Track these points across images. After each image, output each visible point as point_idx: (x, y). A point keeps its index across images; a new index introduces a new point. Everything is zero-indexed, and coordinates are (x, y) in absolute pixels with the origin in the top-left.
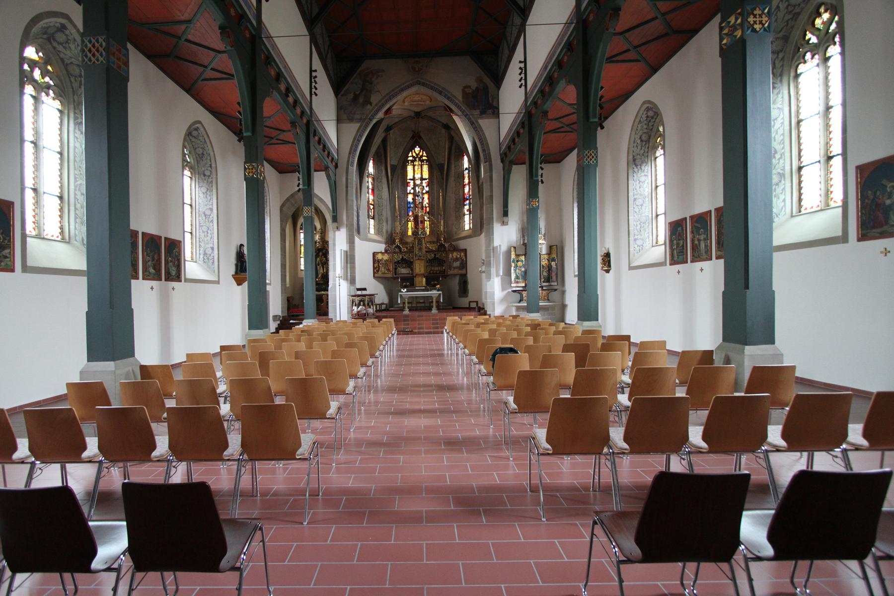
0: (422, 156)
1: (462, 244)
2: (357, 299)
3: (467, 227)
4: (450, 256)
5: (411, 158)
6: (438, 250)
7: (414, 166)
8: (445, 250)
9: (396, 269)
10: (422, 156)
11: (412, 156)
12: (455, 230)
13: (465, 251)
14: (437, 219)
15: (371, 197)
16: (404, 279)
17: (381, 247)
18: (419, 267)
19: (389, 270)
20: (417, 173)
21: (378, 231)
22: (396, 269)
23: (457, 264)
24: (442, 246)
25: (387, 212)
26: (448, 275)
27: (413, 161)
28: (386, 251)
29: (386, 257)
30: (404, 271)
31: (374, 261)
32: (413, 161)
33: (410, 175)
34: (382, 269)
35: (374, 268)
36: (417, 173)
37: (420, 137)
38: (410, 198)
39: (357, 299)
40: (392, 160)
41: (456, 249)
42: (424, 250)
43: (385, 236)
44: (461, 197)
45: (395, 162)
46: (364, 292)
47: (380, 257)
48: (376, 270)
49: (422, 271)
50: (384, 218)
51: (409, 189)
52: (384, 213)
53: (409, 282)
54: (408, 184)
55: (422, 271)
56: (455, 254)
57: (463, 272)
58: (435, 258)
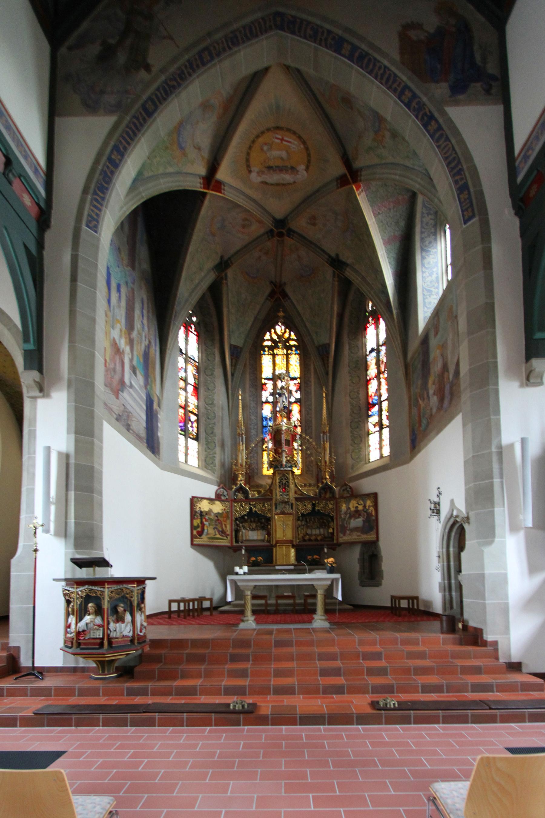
0: (289, 339)
1: (367, 485)
2: (82, 590)
3: (374, 456)
4: (344, 507)
5: (269, 343)
6: (319, 497)
7: (274, 355)
8: (333, 497)
9: (237, 531)
10: (289, 339)
11: (272, 340)
12: (350, 461)
13: (374, 496)
14: (318, 439)
15: (193, 402)
16: (252, 550)
17: (210, 490)
18: (283, 528)
19: (223, 532)
20: (281, 365)
21: (206, 461)
22: (237, 531)
23: (358, 522)
24: (327, 488)
25: (223, 429)
26: (339, 545)
27: (271, 348)
28: (218, 497)
29: (218, 507)
30: (254, 536)
31: (193, 513)
33: (267, 371)
34: (209, 530)
35: (193, 527)
36: (281, 365)
38: (267, 410)
39: (82, 590)
41: (354, 495)
42: (292, 495)
44: (362, 402)
45: (238, 341)
46: (100, 573)
47: (204, 506)
48: (197, 531)
49: (289, 535)
50: (217, 439)
53: (262, 557)
54: (262, 387)
55: (289, 535)
56: (353, 504)
57: (371, 537)
58: (314, 513)
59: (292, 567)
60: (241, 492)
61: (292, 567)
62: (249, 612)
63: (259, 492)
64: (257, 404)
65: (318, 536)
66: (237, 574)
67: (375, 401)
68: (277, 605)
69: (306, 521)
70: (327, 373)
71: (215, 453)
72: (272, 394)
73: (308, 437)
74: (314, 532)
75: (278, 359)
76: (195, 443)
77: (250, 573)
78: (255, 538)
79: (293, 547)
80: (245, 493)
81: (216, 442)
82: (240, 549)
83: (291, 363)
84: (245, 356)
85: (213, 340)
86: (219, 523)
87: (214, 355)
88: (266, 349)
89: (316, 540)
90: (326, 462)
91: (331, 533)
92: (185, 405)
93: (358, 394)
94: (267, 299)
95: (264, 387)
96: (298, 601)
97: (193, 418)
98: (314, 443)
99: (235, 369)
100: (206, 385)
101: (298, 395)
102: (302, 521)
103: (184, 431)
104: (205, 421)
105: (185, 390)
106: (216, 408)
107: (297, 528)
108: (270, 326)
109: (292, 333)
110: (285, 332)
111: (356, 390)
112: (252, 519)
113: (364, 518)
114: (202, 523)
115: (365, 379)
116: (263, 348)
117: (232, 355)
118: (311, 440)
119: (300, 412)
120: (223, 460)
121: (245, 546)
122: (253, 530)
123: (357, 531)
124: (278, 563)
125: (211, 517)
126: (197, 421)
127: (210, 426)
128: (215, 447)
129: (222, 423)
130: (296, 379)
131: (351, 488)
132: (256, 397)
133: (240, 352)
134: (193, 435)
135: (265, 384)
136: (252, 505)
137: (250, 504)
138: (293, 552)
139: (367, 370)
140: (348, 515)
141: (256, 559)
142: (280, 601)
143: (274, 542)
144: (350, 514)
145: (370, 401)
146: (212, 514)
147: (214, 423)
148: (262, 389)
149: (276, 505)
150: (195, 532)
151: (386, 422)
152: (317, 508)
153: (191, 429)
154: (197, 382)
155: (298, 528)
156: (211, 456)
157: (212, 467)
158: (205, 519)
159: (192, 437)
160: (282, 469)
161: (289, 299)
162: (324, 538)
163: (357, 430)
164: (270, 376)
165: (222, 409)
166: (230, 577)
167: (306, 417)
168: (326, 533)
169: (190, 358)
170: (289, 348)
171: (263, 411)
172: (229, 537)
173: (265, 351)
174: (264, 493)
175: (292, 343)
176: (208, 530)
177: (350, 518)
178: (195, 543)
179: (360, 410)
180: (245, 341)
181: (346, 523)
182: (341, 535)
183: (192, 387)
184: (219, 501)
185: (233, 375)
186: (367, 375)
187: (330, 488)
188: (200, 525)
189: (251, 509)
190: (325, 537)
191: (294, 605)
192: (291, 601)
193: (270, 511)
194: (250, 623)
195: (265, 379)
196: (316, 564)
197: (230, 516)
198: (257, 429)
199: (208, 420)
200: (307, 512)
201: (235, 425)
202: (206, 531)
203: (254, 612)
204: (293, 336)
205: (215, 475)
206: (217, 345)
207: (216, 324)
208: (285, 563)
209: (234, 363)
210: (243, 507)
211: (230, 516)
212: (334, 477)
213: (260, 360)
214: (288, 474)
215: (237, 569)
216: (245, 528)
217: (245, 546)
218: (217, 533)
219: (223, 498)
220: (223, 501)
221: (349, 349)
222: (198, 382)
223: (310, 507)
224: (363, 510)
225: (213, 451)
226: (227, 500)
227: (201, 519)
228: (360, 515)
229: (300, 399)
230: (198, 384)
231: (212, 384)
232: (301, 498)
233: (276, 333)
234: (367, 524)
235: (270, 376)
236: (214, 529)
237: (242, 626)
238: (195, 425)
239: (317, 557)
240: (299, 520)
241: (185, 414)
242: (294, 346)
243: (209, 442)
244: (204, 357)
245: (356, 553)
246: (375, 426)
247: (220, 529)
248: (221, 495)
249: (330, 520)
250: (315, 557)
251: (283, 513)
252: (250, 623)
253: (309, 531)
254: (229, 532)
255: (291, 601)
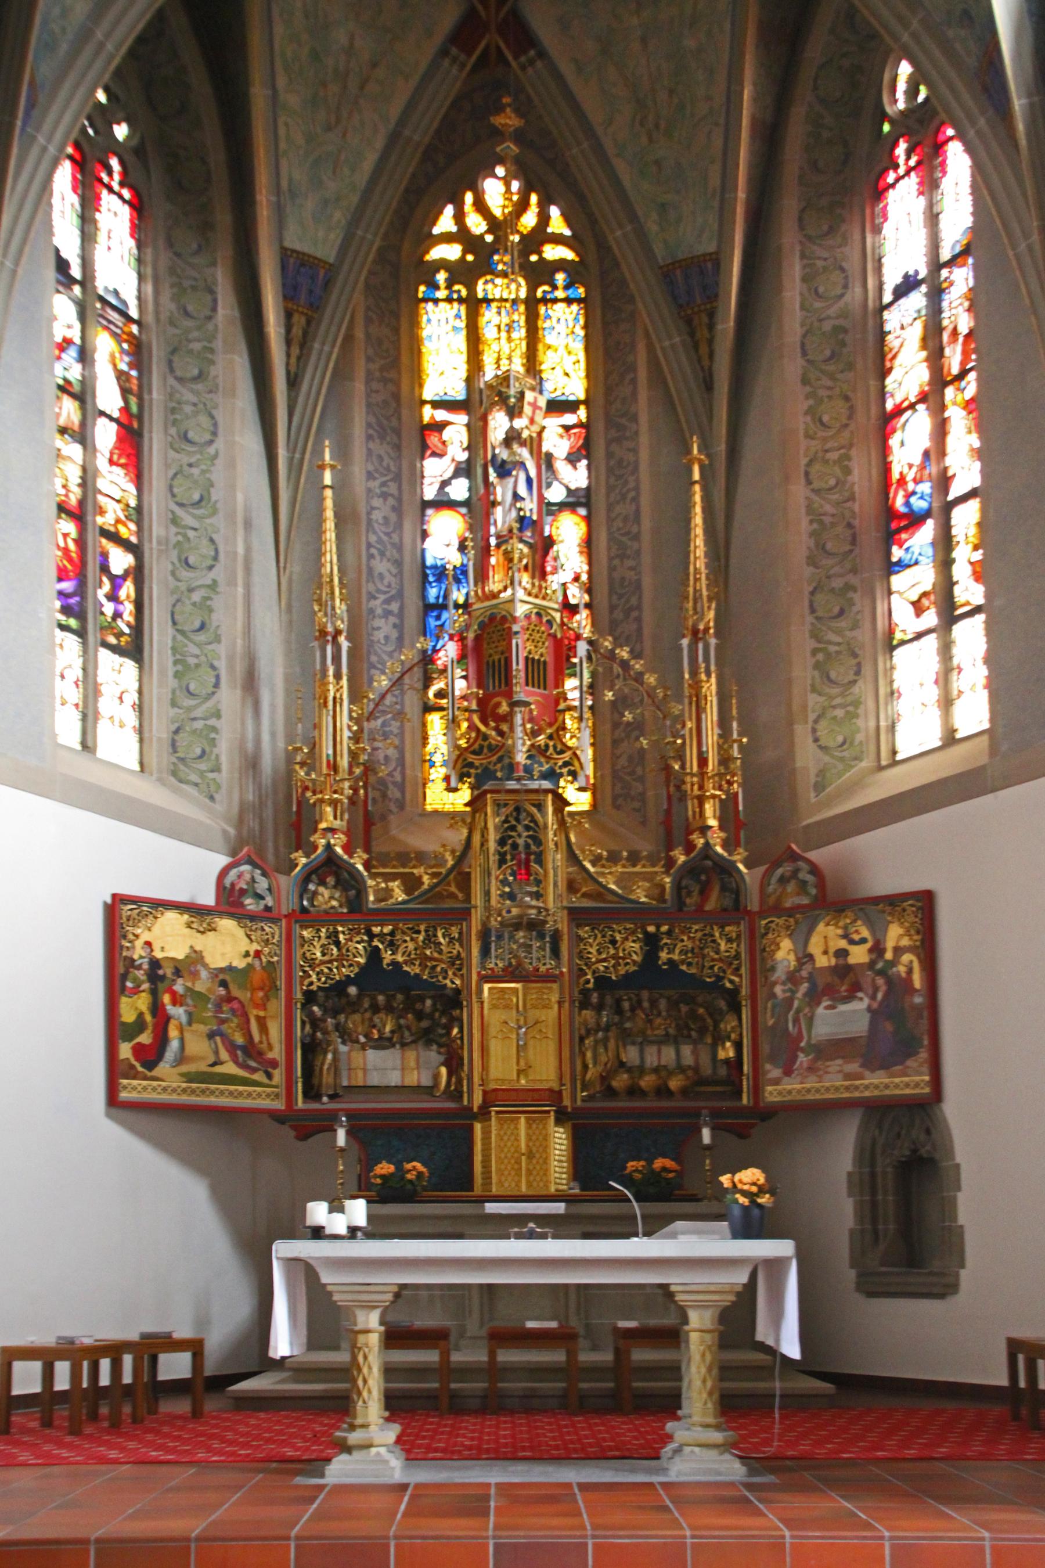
0: (539, 236)
1: (885, 860)
3: (916, 731)
4: (785, 953)
5: (452, 252)
6: (674, 910)
7: (474, 305)
8: (735, 909)
10: (539, 236)
11: (462, 236)
14: (668, 661)
17: (194, 870)
19: (250, 1053)
21: (177, 750)
23: (848, 1017)
24: (708, 871)
26: (765, 1114)
27: (460, 273)
28: (230, 900)
29: (228, 945)
32: (463, 274)
34: (191, 1041)
35: (115, 1030)
36: (505, 351)
37: (523, 38)
38: (444, 538)
40: (303, 211)
41: (832, 900)
42: (553, 901)
43: (228, 801)
44: (865, 503)
48: (133, 1048)
49: (545, 1069)
50: (224, 655)
51: (434, 470)
52: (227, 618)
53: (424, 1164)
54: (427, 438)
55: (545, 1069)
56: (825, 940)
57: (907, 1082)
58: (651, 974)
59: (559, 1208)
60: (331, 880)
61: (559, 1208)
62: (371, 1406)
63: (411, 883)
64: (398, 509)
65: (671, 1074)
66: (317, 1233)
67: (919, 504)
68: (493, 1370)
69: (619, 1011)
70: (708, 385)
71: (218, 715)
72: (464, 470)
73: (624, 653)
74: (651, 1059)
75: (490, 319)
76: (130, 667)
77: (376, 1230)
78: (394, 1078)
79: (558, 1122)
80: (349, 883)
81: (222, 665)
82: (326, 1124)
83: (549, 338)
84: (349, 302)
85: (205, 228)
86: (233, 1011)
87: (212, 292)
88: (441, 277)
89: (663, 1091)
90: (703, 761)
91: (727, 1061)
92: (81, 503)
93: (847, 471)
94: (444, 52)
95: (433, 440)
96: (586, 1357)
97: (120, 561)
98: (651, 679)
99: (303, 358)
100: (175, 423)
101: (578, 477)
102: (599, 1008)
103: (81, 616)
104: (173, 573)
105: (82, 436)
106: (219, 521)
107: (574, 1041)
108: (459, 181)
109: (554, 211)
110: (522, 206)
111: (833, 456)
112: (381, 998)
113: (873, 997)
114: (157, 1008)
115: (874, 411)
116: (427, 272)
117: (289, 294)
118: (638, 666)
119: (588, 545)
120: (250, 746)
121: (351, 1115)
122: (383, 1043)
123: (847, 1058)
124: (495, 1190)
125: (199, 987)
126: (137, 573)
127: (196, 597)
128: (217, 685)
129: (248, 587)
130: (571, 406)
131: (814, 870)
132: (398, 478)
133: (328, 284)
134: (119, 635)
135: (439, 427)
136: (381, 936)
137: (372, 936)
138: (559, 1140)
139: (884, 372)
140: (804, 987)
141: (400, 1171)
142: (507, 1356)
143: (478, 1099)
144: (811, 979)
145: (899, 503)
146: (204, 974)
147: (213, 586)
148: (424, 450)
149: (485, 935)
150: (125, 1051)
151: (969, 591)
152: (664, 955)
153: (109, 608)
154: (134, 409)
155: (582, 1039)
156: (199, 725)
157: (202, 774)
158: (174, 994)
159: (112, 640)
160: (512, 785)
161: (542, 54)
162: (698, 1083)
163: (843, 624)
164: (457, 391)
165: (248, 524)
166: (283, 1249)
167: (612, 569)
168: (705, 1060)
169: (102, 299)
170: (540, 274)
171: (428, 544)
172: (279, 1076)
173: (434, 286)
174: (432, 888)
175: (553, 252)
176: (182, 1040)
177: (814, 997)
178: (124, 1095)
179: (854, 541)
180: (348, 239)
181: (796, 1021)
182: (776, 1073)
183: (114, 426)
184: (232, 915)
185: (293, 382)
186: (882, 395)
187: (725, 869)
188: (148, 1018)
189: (374, 955)
190: (702, 1081)
191: (570, 1371)
192: (557, 1356)
193: (458, 963)
194: (374, 1454)
195: (436, 405)
196: (671, 1198)
197: (282, 983)
198: (401, 614)
199: (184, 574)
200: (622, 970)
201: (304, 592)
202: (174, 1044)
203: (396, 1405)
204: (557, 225)
205: (219, 807)
206: (225, 251)
207: (217, 159)
208: (524, 1189)
209: (297, 331)
210: (337, 943)
211: (282, 983)
212: (739, 825)
213: (414, 323)
214: (540, 806)
215: (318, 1212)
216: (346, 1036)
217: (351, 1115)
218: (224, 1055)
219: (249, 903)
220: (253, 917)
221: (804, 279)
222: (141, 406)
223: (634, 948)
224: (871, 965)
225: (210, 704)
226: (268, 915)
227: (154, 993)
228: (855, 988)
229: (588, 489)
230: (140, 417)
231: (204, 420)
232: (596, 913)
233: (481, 206)
234: (889, 1027)
235: (457, 391)
236: (211, 1036)
237: (340, 1470)
238: (128, 589)
239: (669, 1163)
240: (584, 1004)
241: (80, 542)
242: (561, 265)
243: (187, 667)
244: (166, 298)
245: (839, 1152)
246: (918, 608)
247: (239, 1040)
248: (243, 892)
249: (722, 1004)
250: (659, 1163)
251: (512, 973)
252: (374, 1454)
253: (631, 1055)
254: (277, 1053)
255: (557, 1356)
